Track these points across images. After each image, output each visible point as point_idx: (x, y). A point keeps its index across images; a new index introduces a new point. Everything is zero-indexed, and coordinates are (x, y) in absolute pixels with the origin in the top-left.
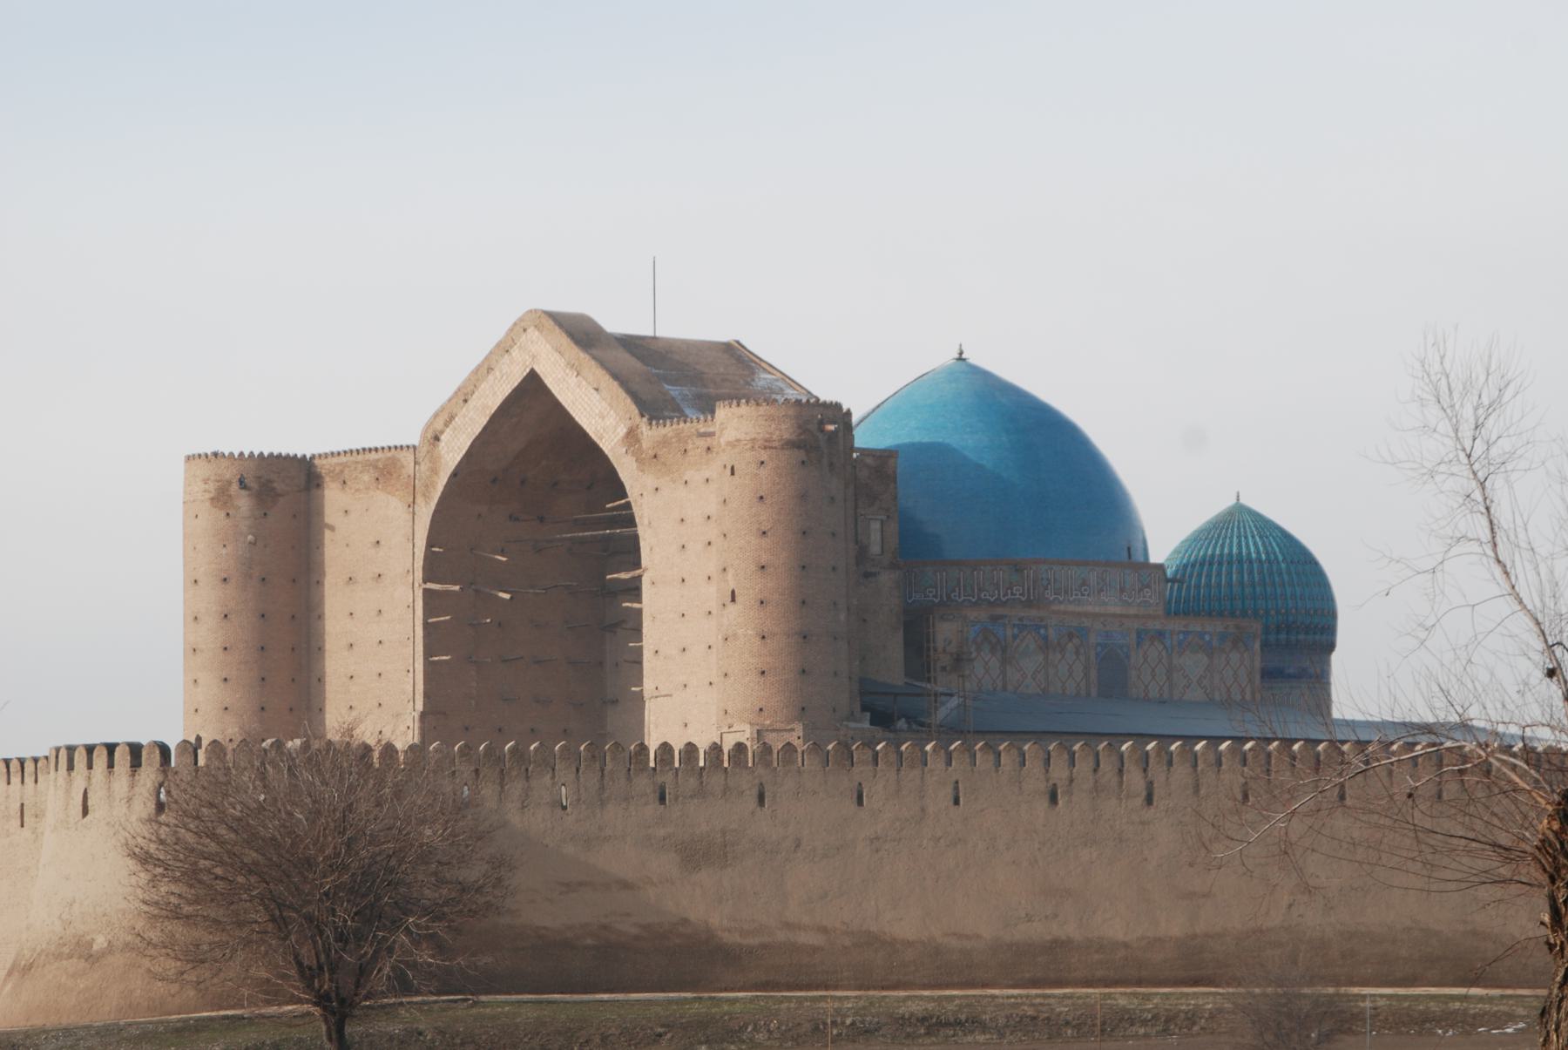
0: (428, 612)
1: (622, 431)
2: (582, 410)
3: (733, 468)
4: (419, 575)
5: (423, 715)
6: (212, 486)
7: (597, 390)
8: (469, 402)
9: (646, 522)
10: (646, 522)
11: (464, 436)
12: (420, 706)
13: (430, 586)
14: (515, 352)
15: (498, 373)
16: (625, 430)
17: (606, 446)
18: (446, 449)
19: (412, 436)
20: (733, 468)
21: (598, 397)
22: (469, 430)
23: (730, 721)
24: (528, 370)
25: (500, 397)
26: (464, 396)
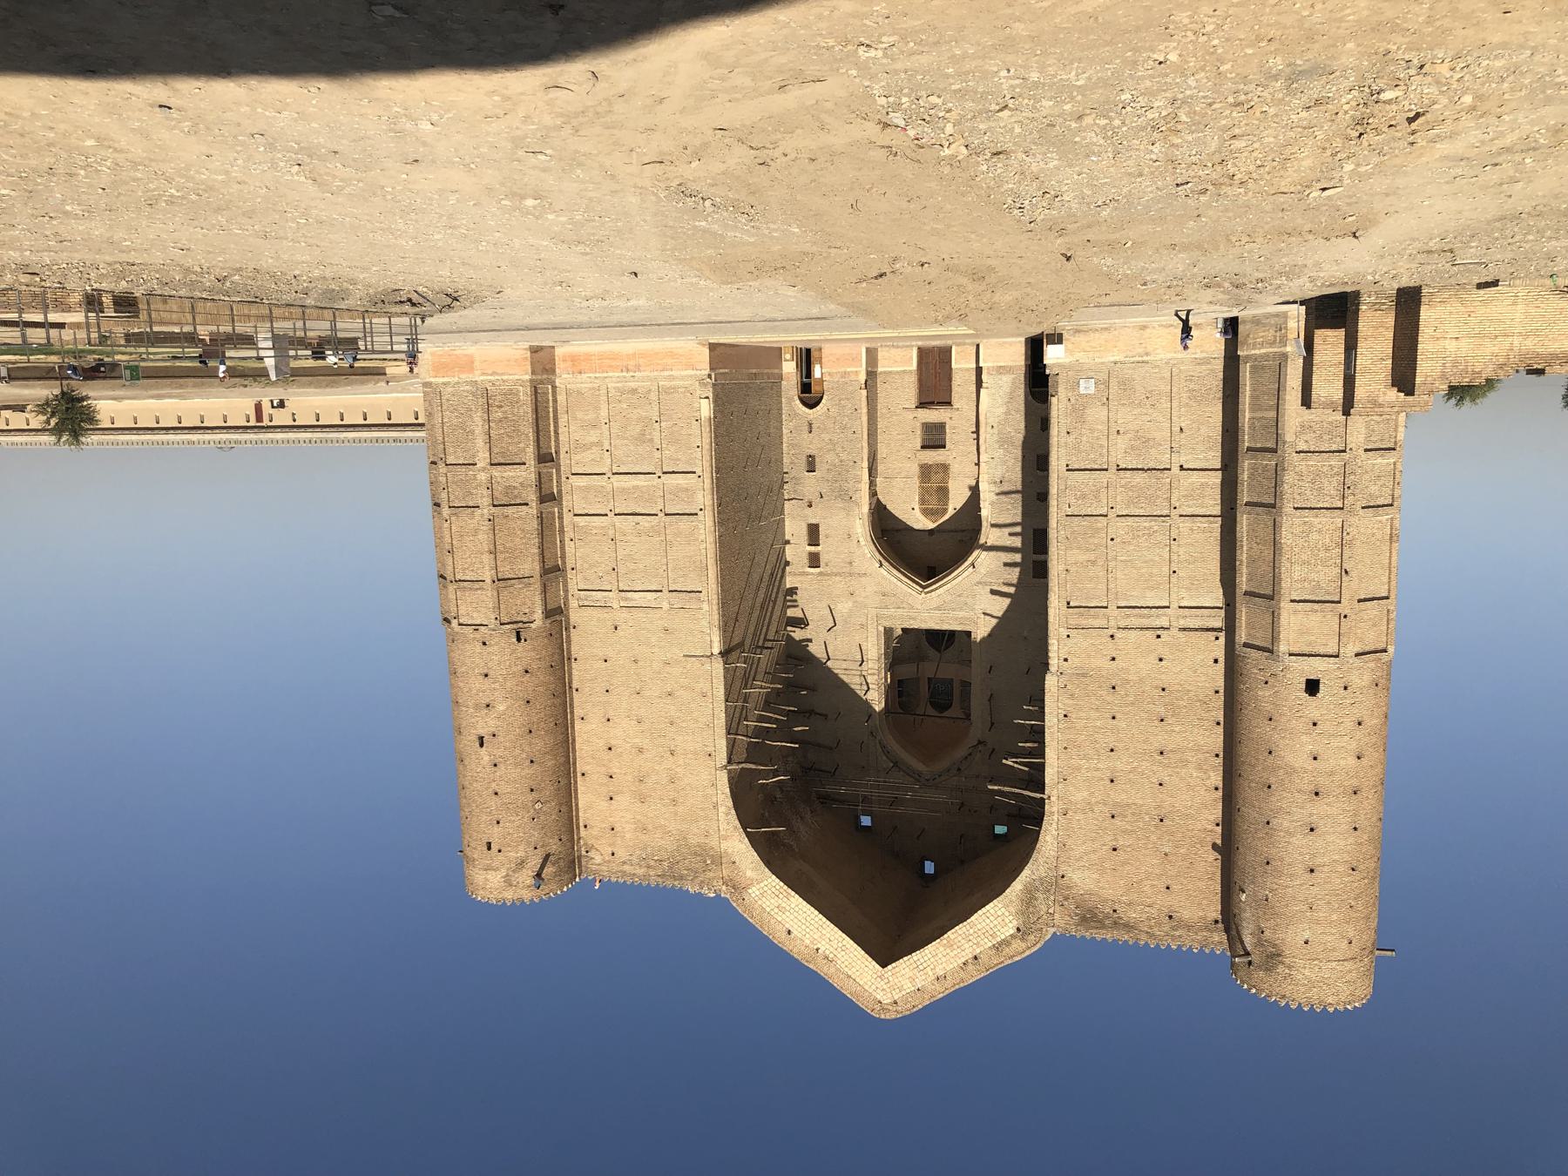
1: (754, 891)
2: (808, 919)
3: (489, 848)
4: (1052, 808)
6: (1280, 969)
8: (970, 956)
9: (722, 809)
11: (979, 926)
12: (1051, 682)
13: (1038, 795)
14: (909, 987)
15: (930, 973)
16: (750, 891)
18: (1007, 921)
20: (489, 848)
21: (787, 926)
22: (971, 931)
23: (477, 635)
24: (890, 967)
25: (927, 951)
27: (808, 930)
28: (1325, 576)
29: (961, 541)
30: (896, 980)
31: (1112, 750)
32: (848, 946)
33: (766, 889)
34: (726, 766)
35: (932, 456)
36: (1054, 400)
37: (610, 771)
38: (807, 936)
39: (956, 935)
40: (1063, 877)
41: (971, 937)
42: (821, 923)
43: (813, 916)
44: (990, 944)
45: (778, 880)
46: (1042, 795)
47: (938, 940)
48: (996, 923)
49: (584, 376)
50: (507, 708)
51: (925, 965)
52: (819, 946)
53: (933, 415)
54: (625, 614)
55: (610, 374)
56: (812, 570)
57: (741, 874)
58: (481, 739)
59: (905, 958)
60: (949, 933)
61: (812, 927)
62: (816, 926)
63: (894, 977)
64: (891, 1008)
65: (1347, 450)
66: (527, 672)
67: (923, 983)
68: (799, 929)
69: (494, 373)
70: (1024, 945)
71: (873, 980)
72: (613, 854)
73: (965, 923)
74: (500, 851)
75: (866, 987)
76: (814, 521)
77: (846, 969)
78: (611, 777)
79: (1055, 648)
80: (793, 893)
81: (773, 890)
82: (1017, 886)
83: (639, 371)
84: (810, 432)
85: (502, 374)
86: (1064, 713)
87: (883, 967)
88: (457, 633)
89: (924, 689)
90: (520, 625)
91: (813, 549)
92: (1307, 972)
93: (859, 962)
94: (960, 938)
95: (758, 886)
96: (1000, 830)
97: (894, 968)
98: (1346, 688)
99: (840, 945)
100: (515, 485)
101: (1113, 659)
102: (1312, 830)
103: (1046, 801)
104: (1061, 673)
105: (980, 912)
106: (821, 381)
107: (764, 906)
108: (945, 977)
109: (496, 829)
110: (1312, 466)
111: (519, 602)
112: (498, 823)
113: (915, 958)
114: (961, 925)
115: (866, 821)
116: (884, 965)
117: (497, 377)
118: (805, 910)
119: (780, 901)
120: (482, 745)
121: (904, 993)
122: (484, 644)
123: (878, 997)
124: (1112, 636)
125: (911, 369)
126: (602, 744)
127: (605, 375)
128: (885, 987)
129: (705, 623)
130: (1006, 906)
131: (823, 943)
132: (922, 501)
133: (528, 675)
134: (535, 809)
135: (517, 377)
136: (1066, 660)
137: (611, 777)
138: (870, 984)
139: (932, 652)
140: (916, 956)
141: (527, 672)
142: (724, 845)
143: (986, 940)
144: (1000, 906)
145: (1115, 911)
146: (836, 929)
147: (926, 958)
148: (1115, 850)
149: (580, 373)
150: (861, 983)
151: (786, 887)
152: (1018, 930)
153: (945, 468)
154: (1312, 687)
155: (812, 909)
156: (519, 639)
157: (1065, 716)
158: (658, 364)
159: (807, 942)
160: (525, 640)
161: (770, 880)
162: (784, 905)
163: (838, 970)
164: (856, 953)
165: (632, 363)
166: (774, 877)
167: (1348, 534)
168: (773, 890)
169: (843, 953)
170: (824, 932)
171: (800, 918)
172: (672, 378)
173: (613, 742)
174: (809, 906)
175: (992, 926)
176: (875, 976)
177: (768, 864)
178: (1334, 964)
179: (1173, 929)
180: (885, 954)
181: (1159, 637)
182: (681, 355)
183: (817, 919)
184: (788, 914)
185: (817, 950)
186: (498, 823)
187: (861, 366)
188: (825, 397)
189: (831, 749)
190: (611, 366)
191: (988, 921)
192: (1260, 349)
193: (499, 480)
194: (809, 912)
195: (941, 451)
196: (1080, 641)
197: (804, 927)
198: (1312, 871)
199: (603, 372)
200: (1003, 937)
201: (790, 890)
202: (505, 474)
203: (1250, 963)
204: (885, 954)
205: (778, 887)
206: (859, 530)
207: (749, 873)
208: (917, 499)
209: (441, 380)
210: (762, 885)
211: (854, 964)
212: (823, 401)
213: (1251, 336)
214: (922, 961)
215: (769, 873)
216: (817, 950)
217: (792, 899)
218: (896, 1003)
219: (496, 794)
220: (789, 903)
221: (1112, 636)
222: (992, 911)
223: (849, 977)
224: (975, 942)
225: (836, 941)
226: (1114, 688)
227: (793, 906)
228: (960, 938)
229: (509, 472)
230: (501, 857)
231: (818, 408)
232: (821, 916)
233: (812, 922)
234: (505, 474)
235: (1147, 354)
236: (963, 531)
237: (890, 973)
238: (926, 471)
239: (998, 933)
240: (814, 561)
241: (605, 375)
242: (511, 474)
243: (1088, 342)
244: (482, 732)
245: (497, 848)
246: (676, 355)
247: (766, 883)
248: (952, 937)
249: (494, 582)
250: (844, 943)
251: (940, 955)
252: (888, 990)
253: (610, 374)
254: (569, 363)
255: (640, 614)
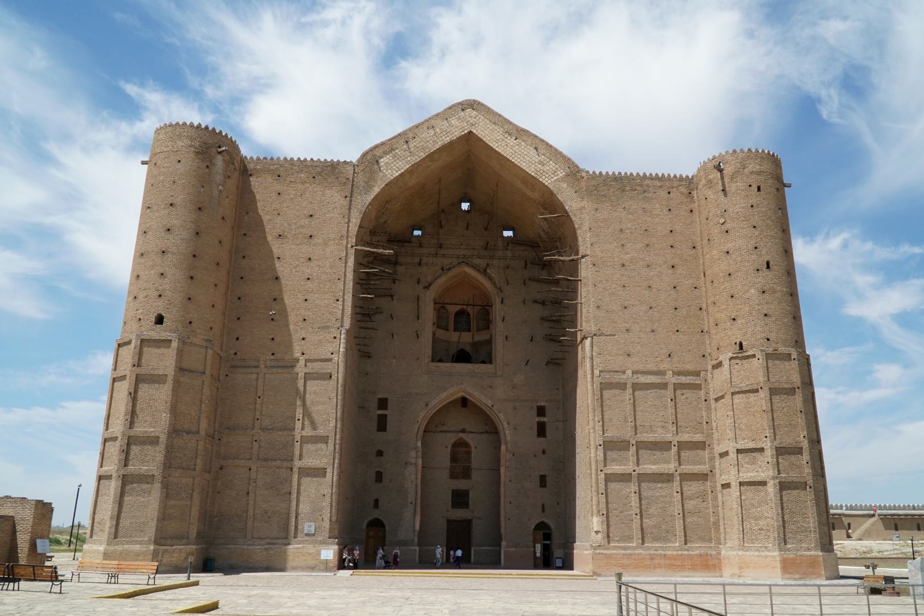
0: (358, 264)
1: (561, 174)
5: (348, 332)
7: (536, 149)
9: (586, 227)
10: (586, 227)
12: (347, 323)
14: (454, 121)
16: (564, 173)
17: (547, 181)
19: (353, 156)
24: (466, 132)
25: (440, 143)
26: (404, 138)
27: (523, 151)
28: (144, 390)
29: (443, 425)
30: (462, 123)
31: (308, 279)
32: (494, 143)
33: (552, 176)
34: (583, 257)
35: (461, 484)
36: (334, 519)
37: (673, 251)
38: (523, 147)
39: (420, 155)
40: (346, 197)
41: (409, 154)
42: (513, 156)
43: (519, 160)
44: (397, 151)
45: (544, 182)
46: (357, 248)
47: (432, 151)
48: (393, 165)
49: (697, 552)
50: (748, 291)
51: (442, 135)
52: (515, 142)
53: (460, 514)
54: (662, 368)
55: (675, 553)
56: (543, 404)
57: (571, 185)
58: (768, 267)
59: (455, 138)
60: (424, 156)
61: (520, 153)
62: (516, 154)
63: (463, 126)
64: (466, 106)
65: (121, 476)
66: (734, 319)
67: (443, 123)
68: (528, 150)
69: (766, 557)
70: (375, 152)
71: (478, 122)
72: (669, 193)
73: (413, 163)
74: (750, 186)
75: (482, 117)
76: (542, 439)
77: (496, 128)
78: (672, 247)
79: (341, 345)
80: (533, 174)
81: (547, 176)
82: (377, 190)
83: (650, 555)
84: (543, 506)
85: (759, 556)
86: (338, 302)
87: (470, 131)
88: (793, 347)
89: (474, 325)
90: (740, 355)
91: (542, 419)
92: (181, 144)
93: (487, 133)
94: (417, 153)
95: (558, 177)
96: (417, 233)
97: (463, 131)
98: (140, 319)
99: (500, 143)
100: (747, 466)
101: (303, 339)
102: (169, 230)
103: (354, 244)
104: (339, 328)
105: (403, 171)
106: (535, 542)
107: (554, 164)
108: (428, 128)
109: (753, 201)
110: (146, 466)
111: (742, 372)
112: (752, 206)
113: (448, 138)
114: (416, 161)
115: (508, 234)
116: (470, 132)
117: (763, 554)
118: (524, 164)
119: (542, 168)
120: (768, 264)
121: (457, 116)
122: (768, 340)
123: (475, 112)
124: (303, 354)
125: (477, 548)
126: (680, 270)
127: (680, 553)
128: (470, 119)
129: (597, 361)
130: (385, 176)
131: (512, 144)
132: (469, 453)
133: (733, 317)
134: (724, 218)
135: (748, 553)
136: (335, 338)
137: (672, 247)
138: (480, 120)
139: (468, 349)
140: (447, 140)
141: (734, 319)
142: (585, 203)
143: (399, 153)
144: (389, 176)
145: (314, 177)
146: (502, 153)
147: (441, 139)
148: (311, 216)
149: (701, 555)
150: (486, 120)
151: (538, 177)
152: (377, 162)
153: (453, 476)
154: (160, 320)
155: (519, 165)
156: (741, 344)
157: (338, 300)
158: (634, 559)
159: (523, 143)
160: (736, 343)
161: (549, 181)
162: (540, 166)
163: (502, 127)
164: (489, 138)
165: (656, 561)
166: (546, 184)
167: (127, 420)
168: (547, 176)
169: (498, 138)
170: (511, 150)
171: (528, 158)
172: (625, 548)
173: (670, 271)
174: (522, 167)
175: (395, 163)
176: (476, 125)
177: (551, 193)
178: (165, 150)
179: (277, 169)
180: (469, 138)
181: (273, 354)
182: (615, 565)
183: (516, 158)
184: (537, 160)
185: (516, 139)
186: (752, 206)
187: (504, 551)
188: (532, 529)
189: (530, 279)
190: (675, 559)
191: (397, 165)
192: (176, 549)
193: (760, 470)
194: (522, 163)
195: (455, 488)
196: (324, 352)
197: (525, 153)
198: (171, 205)
199: (682, 555)
200: (388, 156)
201: (535, 176)
202: (755, 474)
203: (220, 147)
204: (469, 138)
205: (544, 177)
206: (507, 432)
207: (565, 185)
208: (473, 455)
209: (812, 553)
210: (555, 178)
211: (491, 132)
212: (533, 527)
213: (182, 558)
214: (443, 137)
215: (551, 187)
216: (516, 139)
217: (532, 169)
218: (463, 110)
219: (754, 227)
220: (536, 168)
221: (303, 354)
222: (394, 172)
223: (494, 123)
224: (407, 152)
225: (503, 145)
226: (305, 320)
227: (533, 166)
228: (417, 153)
229: (749, 475)
230: (750, 181)
231: (537, 522)
232: (513, 161)
233: (519, 156)
234: (755, 474)
235: (267, 549)
236: (441, 432)
237: (466, 128)
238: (466, 474)
239: (391, 158)
240: (541, 411)
241: (680, 553)
242: (751, 474)
243: (306, 560)
244: (767, 272)
245: (752, 188)
246: (620, 566)
247: (553, 180)
248: (422, 154)
249: (761, 388)
250: (497, 145)
251: (431, 142)
252: (467, 117)
253: (675, 553)
254: (710, 563)
255: (651, 367)
